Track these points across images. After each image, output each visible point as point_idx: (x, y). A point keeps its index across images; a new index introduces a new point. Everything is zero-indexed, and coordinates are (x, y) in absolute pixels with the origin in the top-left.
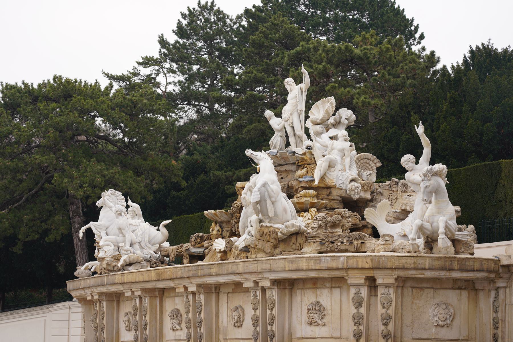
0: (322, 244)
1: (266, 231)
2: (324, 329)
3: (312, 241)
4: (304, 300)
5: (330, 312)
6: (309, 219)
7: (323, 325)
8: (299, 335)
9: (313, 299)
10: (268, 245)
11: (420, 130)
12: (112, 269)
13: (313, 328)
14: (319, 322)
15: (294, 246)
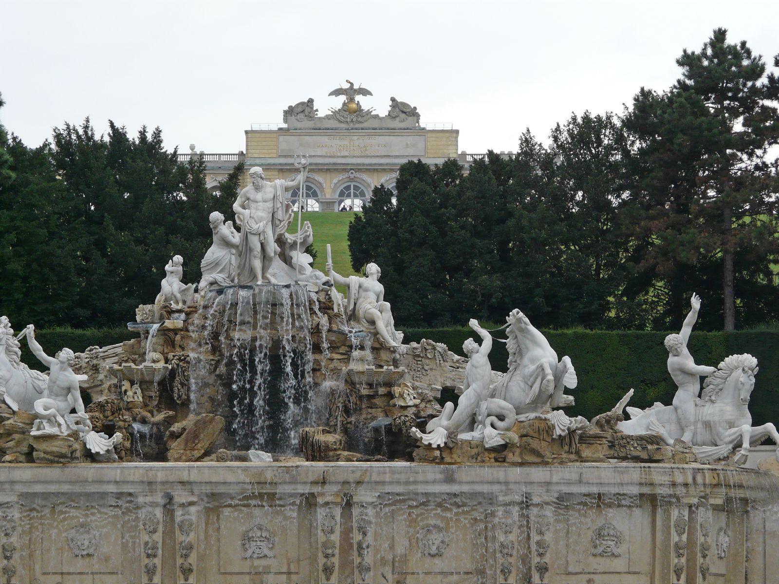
0: (612, 446)
1: (542, 426)
2: (617, 561)
3: (599, 442)
4: (588, 522)
5: (627, 538)
6: (414, 398)
7: (619, 556)
8: (570, 569)
9: (600, 522)
10: (544, 444)
11: (696, 302)
12: (70, 455)
13: (599, 559)
14: (616, 551)
15: (566, 448)
